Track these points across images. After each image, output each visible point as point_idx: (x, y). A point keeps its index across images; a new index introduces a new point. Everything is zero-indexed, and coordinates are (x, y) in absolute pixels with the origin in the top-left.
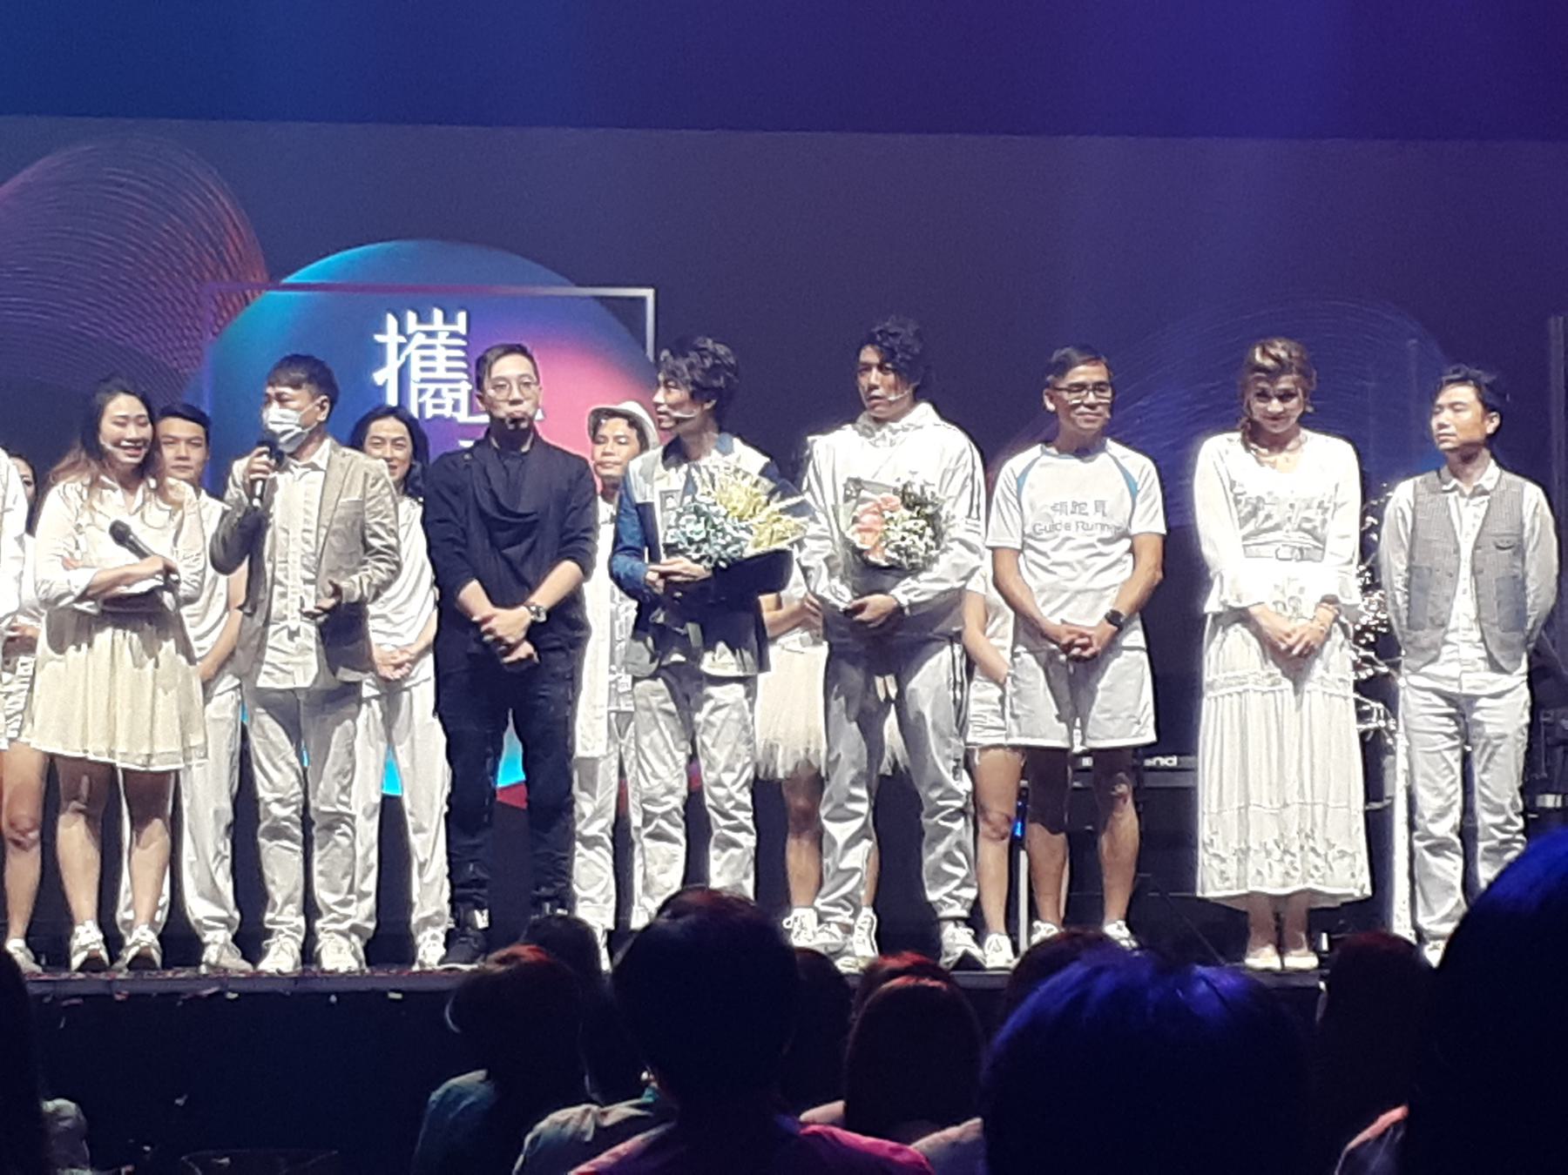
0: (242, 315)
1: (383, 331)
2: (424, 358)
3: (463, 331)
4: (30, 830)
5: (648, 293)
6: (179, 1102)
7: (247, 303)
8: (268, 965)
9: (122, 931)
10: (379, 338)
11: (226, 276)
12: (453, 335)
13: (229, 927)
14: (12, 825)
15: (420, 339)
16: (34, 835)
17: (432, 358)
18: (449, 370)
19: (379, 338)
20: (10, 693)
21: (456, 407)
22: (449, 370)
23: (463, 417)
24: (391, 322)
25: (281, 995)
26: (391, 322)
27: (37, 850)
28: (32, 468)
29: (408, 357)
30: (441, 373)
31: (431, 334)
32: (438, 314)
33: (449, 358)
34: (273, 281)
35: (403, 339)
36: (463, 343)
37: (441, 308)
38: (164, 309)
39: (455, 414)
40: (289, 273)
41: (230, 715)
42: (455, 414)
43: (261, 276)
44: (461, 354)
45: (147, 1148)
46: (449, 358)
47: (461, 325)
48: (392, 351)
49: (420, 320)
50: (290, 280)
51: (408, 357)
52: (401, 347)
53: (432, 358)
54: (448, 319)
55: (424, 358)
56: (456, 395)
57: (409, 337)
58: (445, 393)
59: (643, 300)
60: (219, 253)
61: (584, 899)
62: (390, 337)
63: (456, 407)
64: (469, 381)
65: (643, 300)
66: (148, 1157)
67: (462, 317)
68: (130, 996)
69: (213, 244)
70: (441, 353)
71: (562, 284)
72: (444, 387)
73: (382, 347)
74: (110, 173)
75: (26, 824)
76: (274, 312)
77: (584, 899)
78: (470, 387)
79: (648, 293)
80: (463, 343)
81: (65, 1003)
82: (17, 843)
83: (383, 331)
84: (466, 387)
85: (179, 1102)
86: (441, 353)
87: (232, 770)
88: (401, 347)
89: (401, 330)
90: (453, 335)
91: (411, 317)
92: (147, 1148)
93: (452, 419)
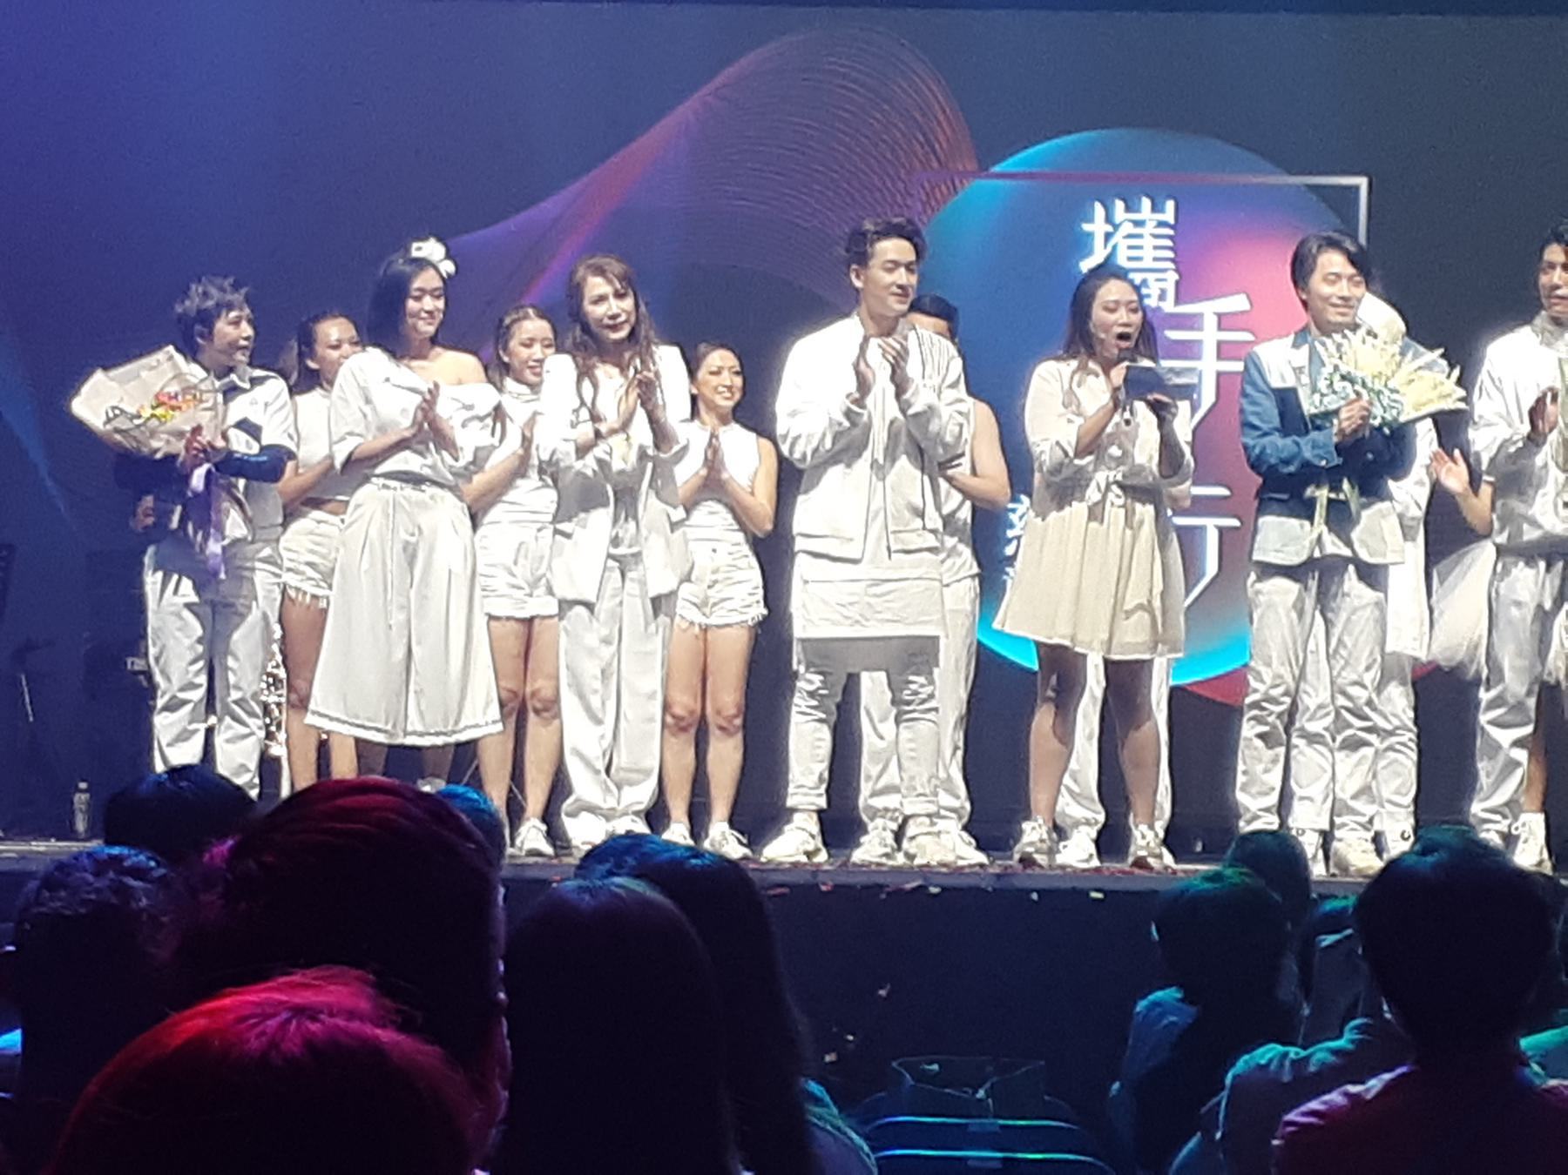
0: (949, 204)
1: (1091, 220)
2: (1130, 247)
3: (1172, 221)
4: (736, 716)
5: (1362, 182)
6: (882, 993)
7: (956, 192)
8: (1060, 859)
9: (865, 818)
10: (1086, 227)
11: (935, 164)
12: (1161, 224)
13: (960, 818)
14: (718, 712)
15: (1128, 228)
16: (738, 722)
17: (1140, 247)
18: (1156, 259)
19: (1086, 227)
20: (716, 582)
21: (1162, 297)
22: (1156, 259)
23: (1169, 306)
24: (1099, 209)
25: (985, 891)
26: (1099, 209)
27: (740, 736)
28: (739, 359)
29: (1114, 247)
30: (1148, 263)
31: (1138, 224)
32: (1146, 203)
33: (1156, 248)
34: (983, 169)
35: (1110, 229)
36: (1171, 232)
37: (1148, 196)
38: (893, 196)
39: (1162, 304)
40: (995, 163)
41: (969, 608)
42: (1162, 304)
43: (972, 166)
44: (1169, 243)
45: (851, 1038)
46: (1156, 248)
47: (1169, 214)
48: (1099, 241)
49: (1128, 209)
50: (997, 169)
51: (1114, 247)
52: (1108, 236)
53: (1140, 247)
54: (1156, 208)
55: (1130, 247)
56: (1162, 285)
57: (1116, 227)
58: (1151, 282)
59: (1356, 188)
60: (928, 140)
61: (1302, 798)
62: (1097, 226)
63: (1162, 297)
64: (1177, 270)
65: (1356, 188)
66: (851, 1046)
67: (1170, 205)
68: (836, 886)
69: (924, 135)
70: (1148, 242)
71: (1272, 173)
72: (1151, 277)
73: (1090, 235)
74: (830, 63)
75: (733, 711)
76: (982, 200)
77: (1302, 798)
78: (1176, 277)
79: (1362, 182)
80: (1171, 232)
81: (772, 892)
82: (721, 728)
83: (1091, 220)
84: (1173, 277)
85: (882, 993)
86: (1148, 242)
87: (968, 665)
88: (1108, 236)
89: (1109, 219)
90: (1161, 224)
91: (1119, 205)
92: (851, 1038)
93: (1158, 309)
